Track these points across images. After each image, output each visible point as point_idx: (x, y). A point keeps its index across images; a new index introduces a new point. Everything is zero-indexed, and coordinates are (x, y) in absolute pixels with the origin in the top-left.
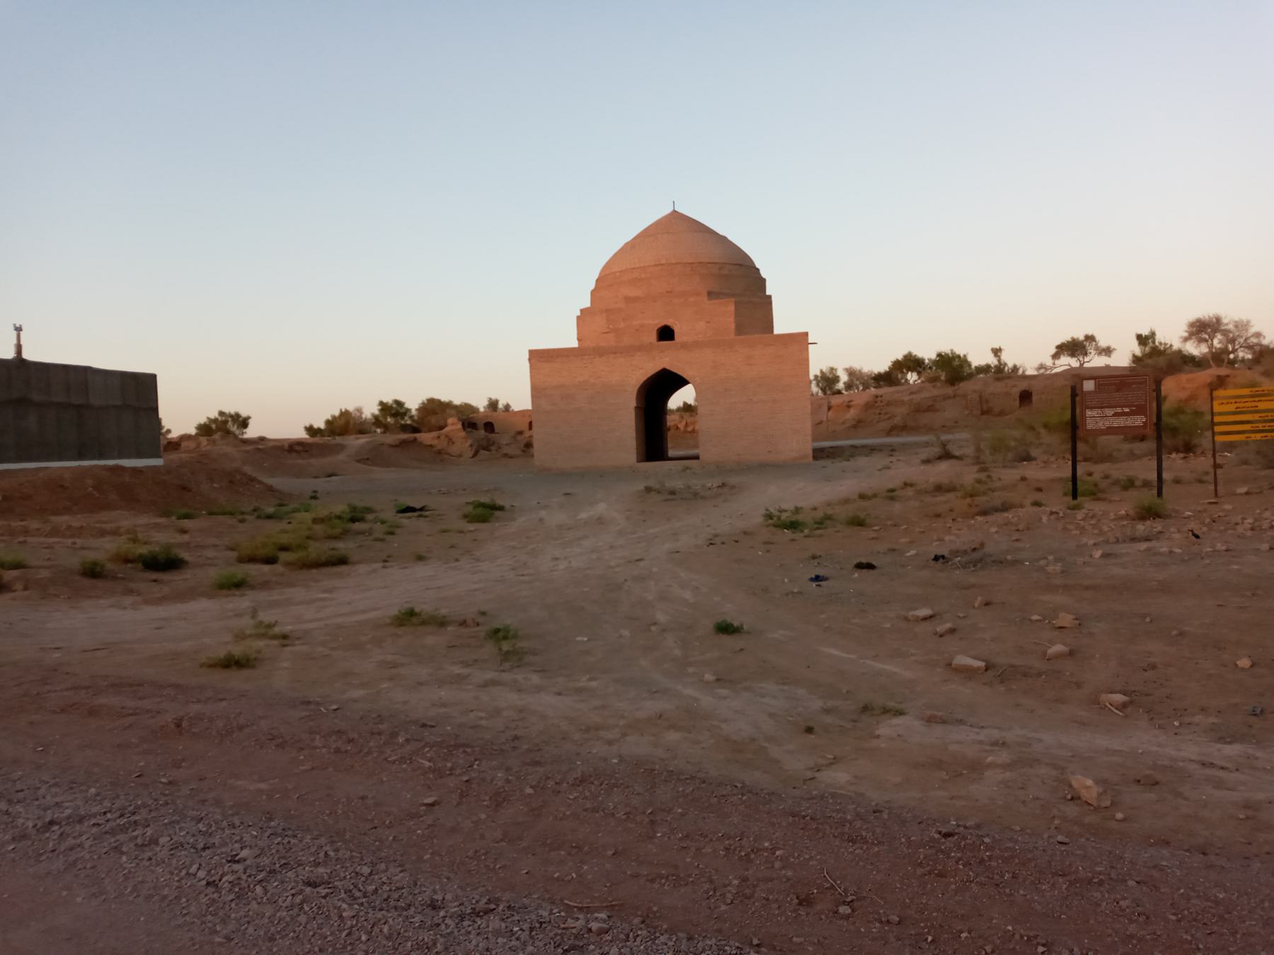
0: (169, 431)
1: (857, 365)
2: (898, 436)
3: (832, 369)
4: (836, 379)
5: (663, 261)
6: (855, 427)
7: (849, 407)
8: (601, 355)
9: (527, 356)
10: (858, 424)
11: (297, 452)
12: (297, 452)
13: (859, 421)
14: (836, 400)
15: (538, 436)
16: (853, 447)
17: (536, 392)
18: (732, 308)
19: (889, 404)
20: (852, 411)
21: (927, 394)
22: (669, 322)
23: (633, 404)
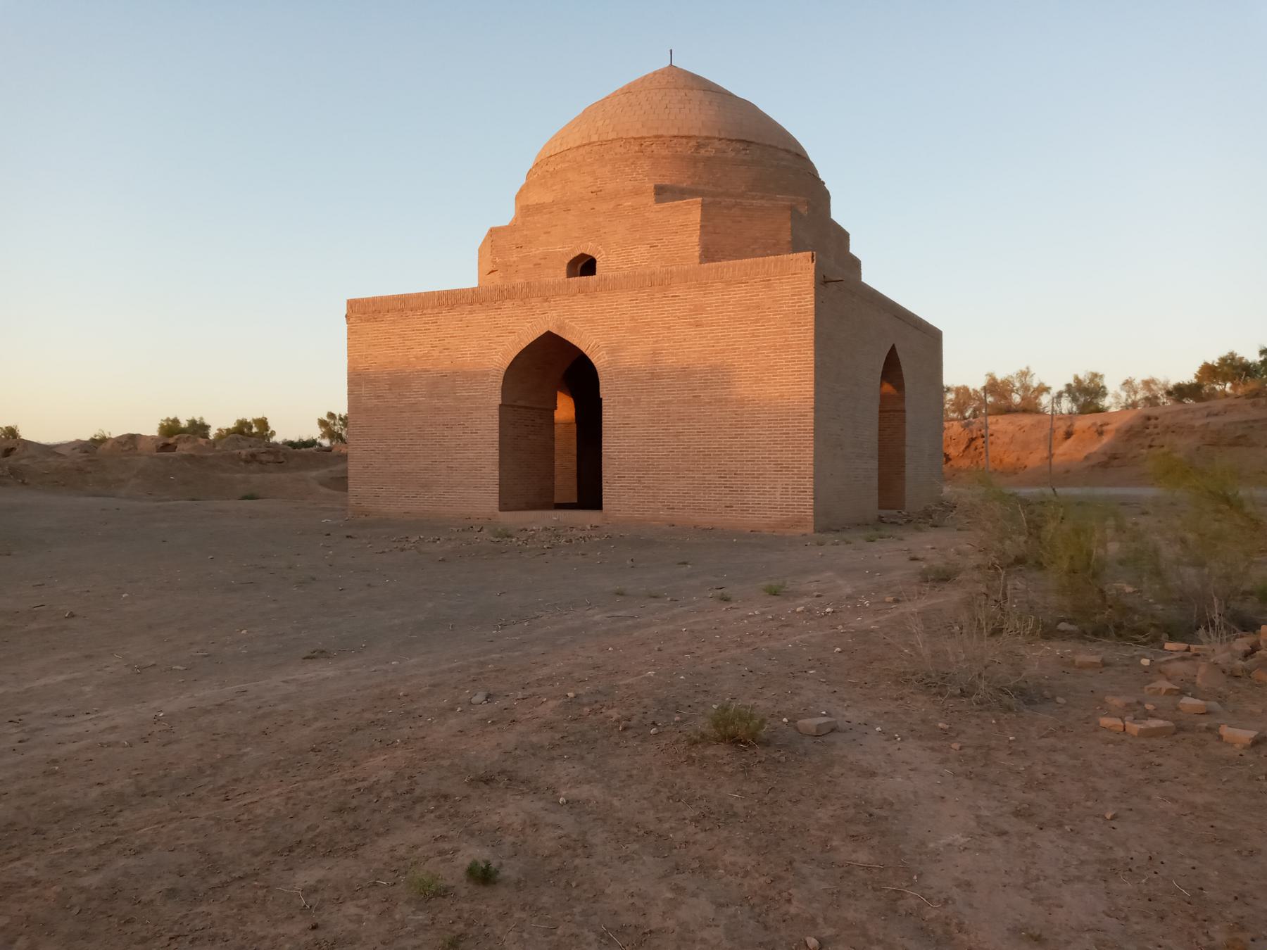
0: (273, 433)
3: (1095, 375)
4: (1100, 392)
5: (595, 138)
6: (1104, 465)
7: (1101, 433)
8: (452, 307)
10: (1109, 463)
11: (261, 462)
12: (261, 462)
13: (1114, 457)
17: (356, 380)
18: (696, 215)
19: (1170, 430)
20: (1106, 439)
21: (1236, 417)
23: (497, 400)
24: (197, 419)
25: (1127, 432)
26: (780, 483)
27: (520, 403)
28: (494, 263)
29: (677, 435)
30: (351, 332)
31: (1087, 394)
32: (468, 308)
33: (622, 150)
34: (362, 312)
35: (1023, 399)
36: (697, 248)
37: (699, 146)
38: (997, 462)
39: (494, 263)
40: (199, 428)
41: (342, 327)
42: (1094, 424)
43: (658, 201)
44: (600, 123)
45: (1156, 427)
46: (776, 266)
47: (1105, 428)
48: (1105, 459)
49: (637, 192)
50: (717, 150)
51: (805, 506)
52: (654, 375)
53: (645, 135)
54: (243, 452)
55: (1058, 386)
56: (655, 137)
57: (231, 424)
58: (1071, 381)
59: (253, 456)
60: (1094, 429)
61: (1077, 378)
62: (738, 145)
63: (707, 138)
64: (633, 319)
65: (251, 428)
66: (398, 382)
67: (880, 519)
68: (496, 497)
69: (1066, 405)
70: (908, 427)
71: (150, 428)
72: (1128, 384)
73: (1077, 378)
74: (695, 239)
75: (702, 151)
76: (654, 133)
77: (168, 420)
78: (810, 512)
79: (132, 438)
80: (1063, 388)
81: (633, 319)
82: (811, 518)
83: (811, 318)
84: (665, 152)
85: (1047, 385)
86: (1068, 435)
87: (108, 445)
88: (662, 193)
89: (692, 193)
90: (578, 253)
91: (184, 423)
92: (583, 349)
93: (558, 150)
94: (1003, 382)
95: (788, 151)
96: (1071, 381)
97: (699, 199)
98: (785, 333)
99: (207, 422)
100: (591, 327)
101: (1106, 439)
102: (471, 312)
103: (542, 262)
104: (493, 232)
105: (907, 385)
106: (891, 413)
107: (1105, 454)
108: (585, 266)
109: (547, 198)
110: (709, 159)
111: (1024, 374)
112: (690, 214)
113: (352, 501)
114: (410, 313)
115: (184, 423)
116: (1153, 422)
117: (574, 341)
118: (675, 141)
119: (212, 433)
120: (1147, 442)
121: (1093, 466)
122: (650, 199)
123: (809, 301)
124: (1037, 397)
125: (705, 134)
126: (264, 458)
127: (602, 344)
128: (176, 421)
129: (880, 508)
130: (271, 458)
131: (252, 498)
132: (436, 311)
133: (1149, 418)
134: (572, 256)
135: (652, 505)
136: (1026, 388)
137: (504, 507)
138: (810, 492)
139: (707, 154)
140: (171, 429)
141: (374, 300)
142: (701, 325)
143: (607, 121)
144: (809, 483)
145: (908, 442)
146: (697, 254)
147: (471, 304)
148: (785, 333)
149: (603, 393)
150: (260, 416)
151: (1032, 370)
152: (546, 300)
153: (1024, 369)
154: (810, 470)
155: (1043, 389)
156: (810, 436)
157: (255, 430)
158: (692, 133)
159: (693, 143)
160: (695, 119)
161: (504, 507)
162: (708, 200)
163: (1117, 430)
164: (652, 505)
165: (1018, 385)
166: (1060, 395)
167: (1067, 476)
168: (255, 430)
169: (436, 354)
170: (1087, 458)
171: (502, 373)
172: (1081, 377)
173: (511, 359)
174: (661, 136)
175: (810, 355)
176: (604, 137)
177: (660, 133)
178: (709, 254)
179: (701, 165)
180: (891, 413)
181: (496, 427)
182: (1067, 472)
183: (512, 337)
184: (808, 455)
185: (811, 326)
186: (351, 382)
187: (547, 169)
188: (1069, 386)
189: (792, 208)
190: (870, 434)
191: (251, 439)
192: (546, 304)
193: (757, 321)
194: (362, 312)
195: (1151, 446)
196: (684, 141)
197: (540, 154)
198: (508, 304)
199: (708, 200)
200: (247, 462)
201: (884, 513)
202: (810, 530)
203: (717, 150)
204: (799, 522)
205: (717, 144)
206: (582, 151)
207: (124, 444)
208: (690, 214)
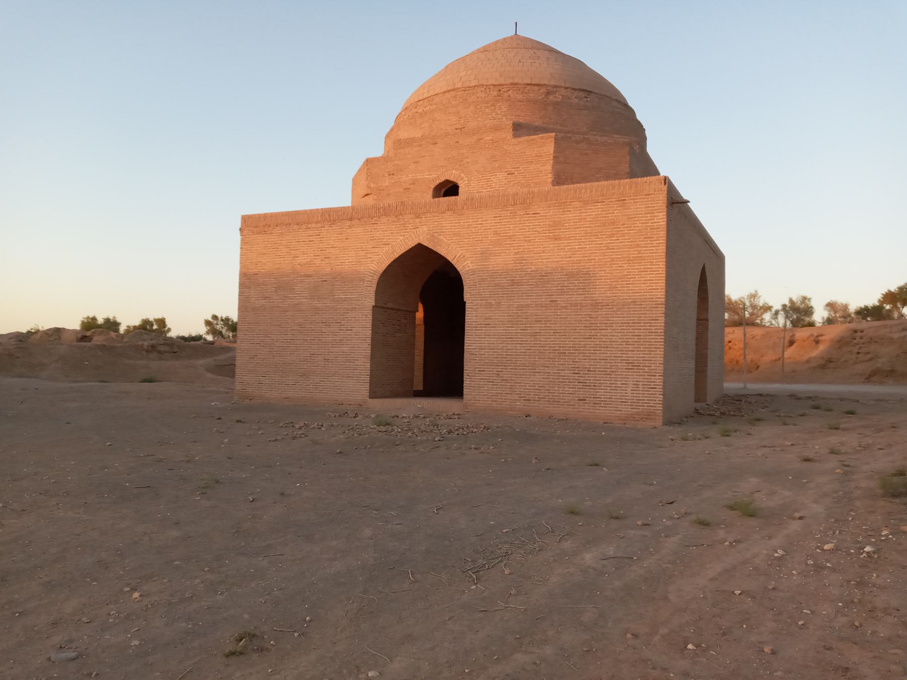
0: (169, 330)
1: (840, 299)
2: (881, 383)
3: (805, 298)
4: (809, 311)
5: (459, 85)
6: (823, 367)
7: (817, 342)
8: (333, 222)
9: (238, 224)
10: (826, 366)
11: (159, 352)
13: (830, 361)
14: (802, 334)
15: (243, 348)
16: (794, 396)
17: (247, 281)
19: (871, 340)
20: (822, 347)
22: (452, 175)
23: (371, 302)
24: (111, 318)
25: (839, 341)
26: (634, 379)
27: (390, 305)
28: (369, 187)
29: (534, 335)
30: (243, 242)
31: (799, 312)
32: (348, 223)
33: (483, 95)
34: (254, 226)
35: (751, 314)
36: (550, 175)
37: (548, 93)
38: (734, 363)
39: (369, 187)
40: (111, 325)
41: (236, 238)
42: (812, 335)
43: (515, 136)
44: (463, 74)
45: (861, 338)
46: (631, 188)
47: (821, 338)
48: (822, 362)
49: (496, 129)
50: (563, 97)
51: (655, 401)
52: (513, 283)
53: (502, 82)
54: (146, 344)
55: (777, 306)
56: (511, 84)
57: (137, 322)
58: (787, 303)
59: (153, 346)
60: (812, 338)
61: (791, 301)
62: (581, 94)
63: (555, 86)
64: (496, 233)
65: (152, 325)
66: (283, 284)
67: (697, 411)
68: (367, 386)
69: (781, 320)
70: (710, 334)
71: (74, 324)
72: (831, 306)
73: (791, 301)
74: (549, 167)
75: (551, 97)
76: (511, 81)
77: (88, 318)
78: (660, 407)
79: (58, 331)
80: (779, 307)
81: (496, 233)
82: (660, 413)
83: (663, 233)
84: (520, 97)
85: (770, 304)
86: (791, 343)
87: (38, 336)
88: (519, 129)
89: (545, 130)
90: (443, 179)
91: (100, 321)
92: (450, 258)
93: (426, 95)
94: (736, 302)
95: (619, 101)
96: (787, 303)
97: (553, 134)
98: (638, 246)
99: (118, 320)
100: (459, 241)
101: (822, 347)
102: (350, 227)
103: (412, 187)
104: (369, 162)
105: (710, 299)
106: (702, 322)
107: (822, 358)
108: (449, 189)
109: (418, 134)
110: (557, 103)
111: (754, 296)
112: (544, 147)
113: (238, 387)
114: (296, 227)
115: (100, 321)
116: (859, 334)
117: (443, 252)
118: (528, 87)
119: (122, 329)
120: (856, 350)
121: (814, 368)
122: (509, 134)
123: (661, 219)
124: (762, 314)
125: (553, 83)
126: (162, 348)
127: (467, 255)
128: (94, 319)
129: (696, 401)
130: (167, 349)
131: (150, 381)
132: (320, 225)
133: (856, 331)
134: (438, 182)
135: (509, 397)
136: (754, 307)
137: (373, 395)
138: (659, 389)
139: (555, 100)
140: (90, 325)
141: (265, 216)
142: (560, 239)
143: (470, 72)
144: (659, 381)
145: (709, 347)
146: (550, 180)
147: (351, 220)
148: (638, 246)
149: (467, 297)
150: (160, 317)
151: (760, 294)
152: (418, 217)
153: (753, 292)
154: (660, 369)
155: (767, 308)
156: (660, 339)
157: (155, 327)
158: (542, 82)
159: (543, 90)
160: (545, 73)
161: (373, 395)
162: (560, 135)
163: (832, 340)
164: (509, 397)
165: (748, 304)
166: (777, 313)
167: (792, 375)
168: (155, 327)
169: (317, 262)
170: (808, 361)
171: (376, 278)
172: (794, 299)
173: (384, 267)
174: (517, 84)
175: (662, 265)
176: (468, 84)
177: (516, 81)
178: (559, 180)
179: (551, 108)
180: (702, 322)
181: (369, 325)
182: (794, 371)
183: (386, 248)
184: (659, 355)
185: (663, 241)
186: (241, 285)
187: (413, 112)
188: (784, 306)
189: (629, 144)
190: (692, 336)
191: (152, 333)
192: (418, 220)
193: (612, 236)
194: (254, 226)
195: (858, 353)
196: (536, 88)
197: (407, 102)
198: (384, 219)
199: (560, 135)
200: (148, 351)
201: (698, 405)
202: (659, 422)
203: (563, 97)
204: (649, 416)
205: (563, 91)
206: (448, 95)
207: (50, 336)
208: (546, 146)
